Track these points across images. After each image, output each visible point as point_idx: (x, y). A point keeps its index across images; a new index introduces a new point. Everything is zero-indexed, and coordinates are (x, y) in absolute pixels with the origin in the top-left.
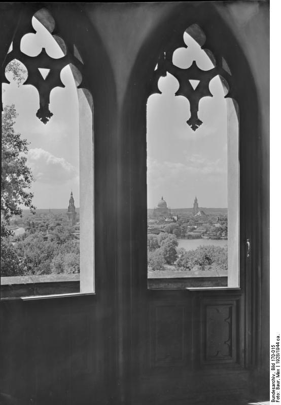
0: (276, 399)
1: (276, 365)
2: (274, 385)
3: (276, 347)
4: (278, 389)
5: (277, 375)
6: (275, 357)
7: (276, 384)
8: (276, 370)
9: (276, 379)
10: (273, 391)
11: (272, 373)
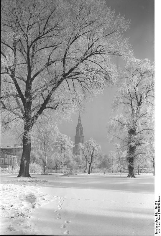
0: (158, 232)
1: (158, 213)
2: (157, 224)
3: (158, 202)
4: (159, 226)
5: (159, 219)
6: (158, 208)
7: (158, 224)
8: (158, 216)
9: (158, 221)
10: (157, 228)
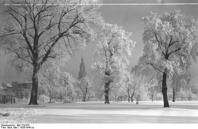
1: (20, 127)
2: (10, 125)
4: (8, 128)
5: (14, 127)
6: (24, 126)
7: (10, 127)
8: (17, 127)
9: (13, 127)
10: (7, 125)
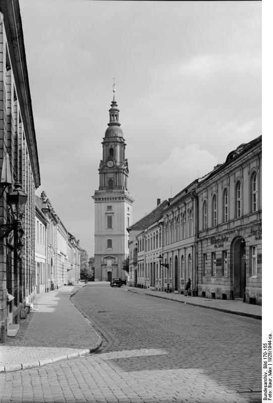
1: (268, 363)
2: (266, 383)
3: (268, 345)
4: (270, 387)
6: (267, 355)
7: (268, 382)
9: (268, 377)
10: (266, 389)
11: (264, 371)
